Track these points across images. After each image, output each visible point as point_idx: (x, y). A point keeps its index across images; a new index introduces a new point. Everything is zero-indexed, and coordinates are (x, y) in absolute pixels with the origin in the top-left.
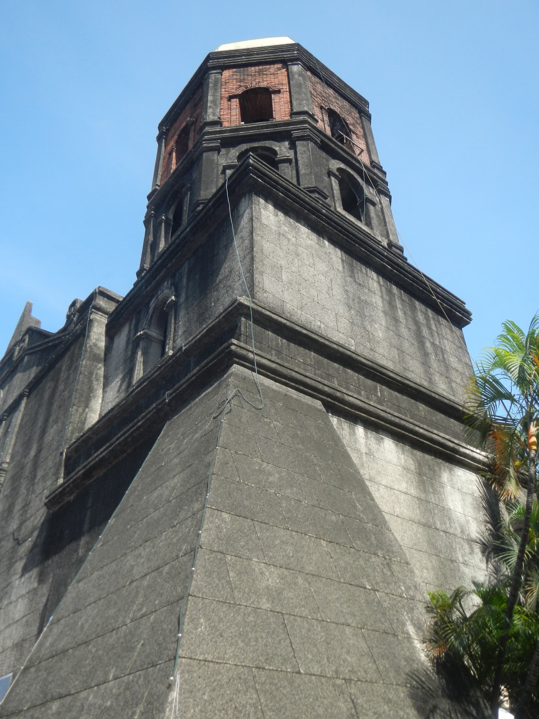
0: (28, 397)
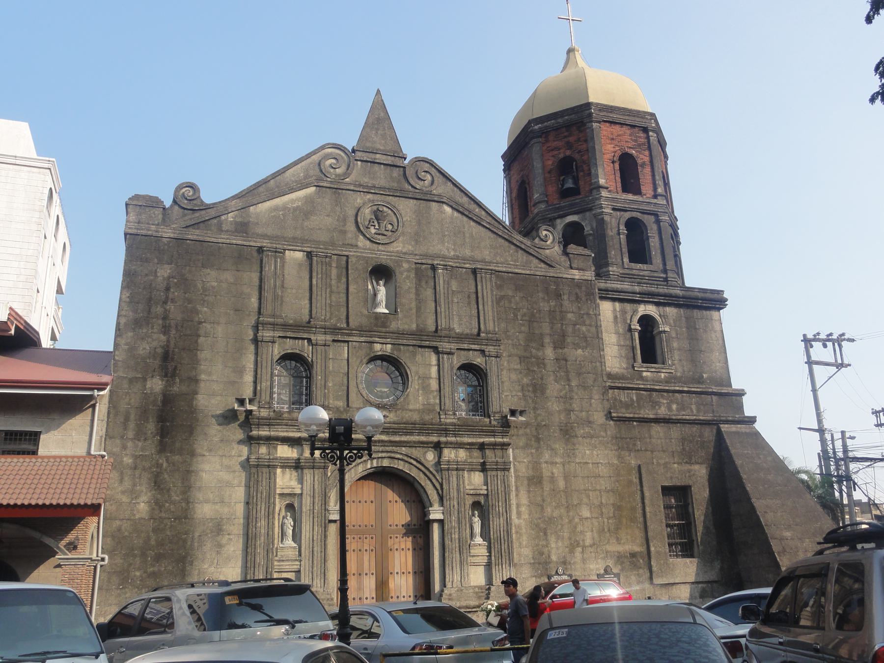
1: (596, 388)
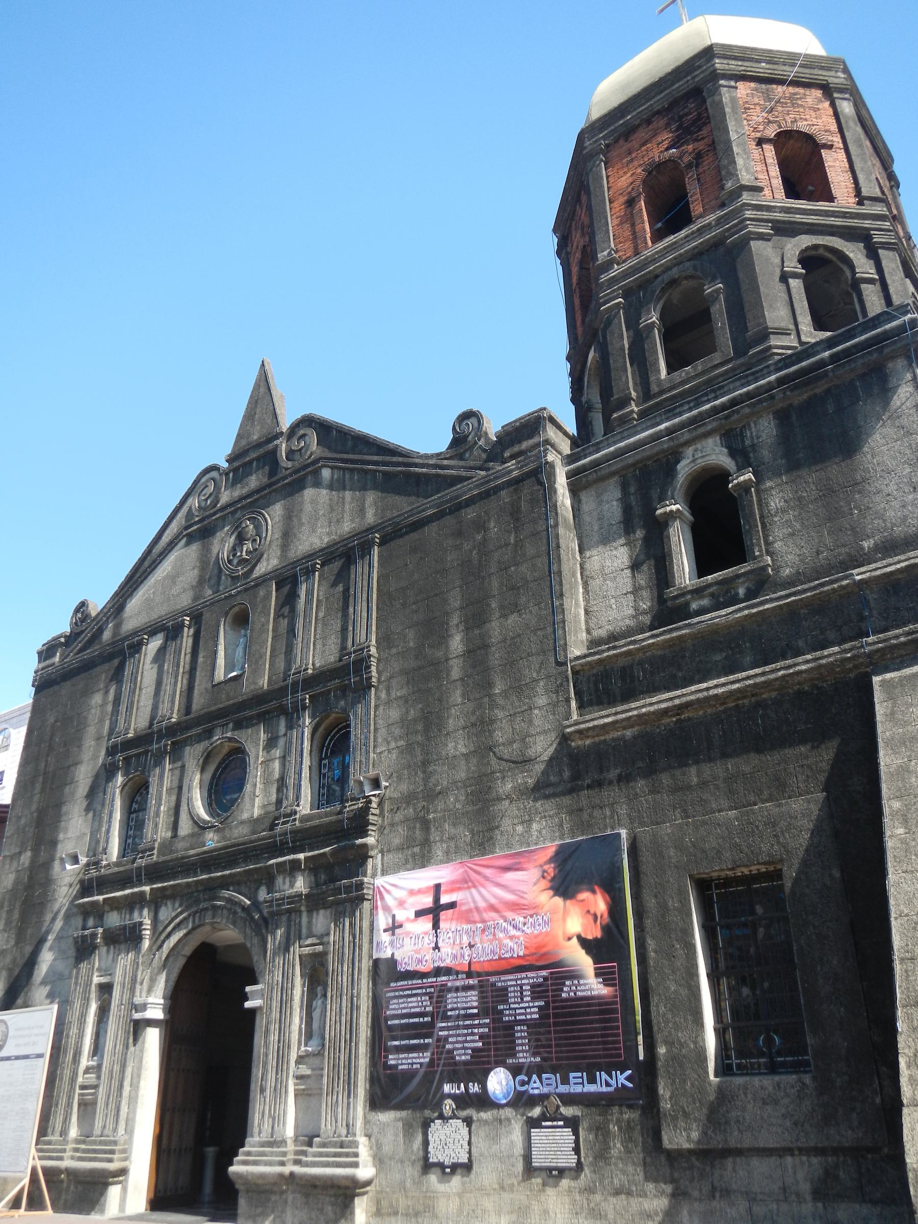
0: (380, 545)
1: (542, 683)
